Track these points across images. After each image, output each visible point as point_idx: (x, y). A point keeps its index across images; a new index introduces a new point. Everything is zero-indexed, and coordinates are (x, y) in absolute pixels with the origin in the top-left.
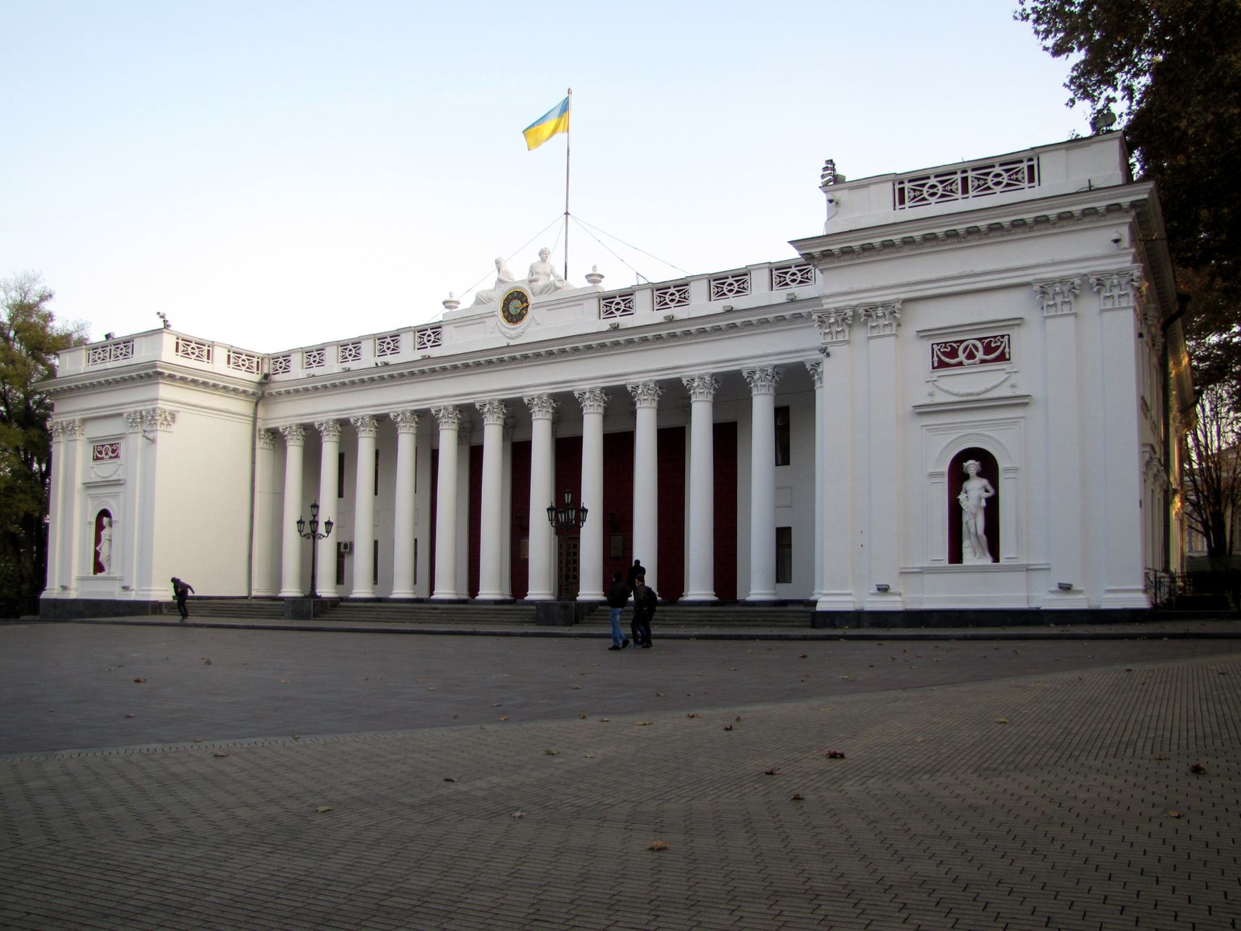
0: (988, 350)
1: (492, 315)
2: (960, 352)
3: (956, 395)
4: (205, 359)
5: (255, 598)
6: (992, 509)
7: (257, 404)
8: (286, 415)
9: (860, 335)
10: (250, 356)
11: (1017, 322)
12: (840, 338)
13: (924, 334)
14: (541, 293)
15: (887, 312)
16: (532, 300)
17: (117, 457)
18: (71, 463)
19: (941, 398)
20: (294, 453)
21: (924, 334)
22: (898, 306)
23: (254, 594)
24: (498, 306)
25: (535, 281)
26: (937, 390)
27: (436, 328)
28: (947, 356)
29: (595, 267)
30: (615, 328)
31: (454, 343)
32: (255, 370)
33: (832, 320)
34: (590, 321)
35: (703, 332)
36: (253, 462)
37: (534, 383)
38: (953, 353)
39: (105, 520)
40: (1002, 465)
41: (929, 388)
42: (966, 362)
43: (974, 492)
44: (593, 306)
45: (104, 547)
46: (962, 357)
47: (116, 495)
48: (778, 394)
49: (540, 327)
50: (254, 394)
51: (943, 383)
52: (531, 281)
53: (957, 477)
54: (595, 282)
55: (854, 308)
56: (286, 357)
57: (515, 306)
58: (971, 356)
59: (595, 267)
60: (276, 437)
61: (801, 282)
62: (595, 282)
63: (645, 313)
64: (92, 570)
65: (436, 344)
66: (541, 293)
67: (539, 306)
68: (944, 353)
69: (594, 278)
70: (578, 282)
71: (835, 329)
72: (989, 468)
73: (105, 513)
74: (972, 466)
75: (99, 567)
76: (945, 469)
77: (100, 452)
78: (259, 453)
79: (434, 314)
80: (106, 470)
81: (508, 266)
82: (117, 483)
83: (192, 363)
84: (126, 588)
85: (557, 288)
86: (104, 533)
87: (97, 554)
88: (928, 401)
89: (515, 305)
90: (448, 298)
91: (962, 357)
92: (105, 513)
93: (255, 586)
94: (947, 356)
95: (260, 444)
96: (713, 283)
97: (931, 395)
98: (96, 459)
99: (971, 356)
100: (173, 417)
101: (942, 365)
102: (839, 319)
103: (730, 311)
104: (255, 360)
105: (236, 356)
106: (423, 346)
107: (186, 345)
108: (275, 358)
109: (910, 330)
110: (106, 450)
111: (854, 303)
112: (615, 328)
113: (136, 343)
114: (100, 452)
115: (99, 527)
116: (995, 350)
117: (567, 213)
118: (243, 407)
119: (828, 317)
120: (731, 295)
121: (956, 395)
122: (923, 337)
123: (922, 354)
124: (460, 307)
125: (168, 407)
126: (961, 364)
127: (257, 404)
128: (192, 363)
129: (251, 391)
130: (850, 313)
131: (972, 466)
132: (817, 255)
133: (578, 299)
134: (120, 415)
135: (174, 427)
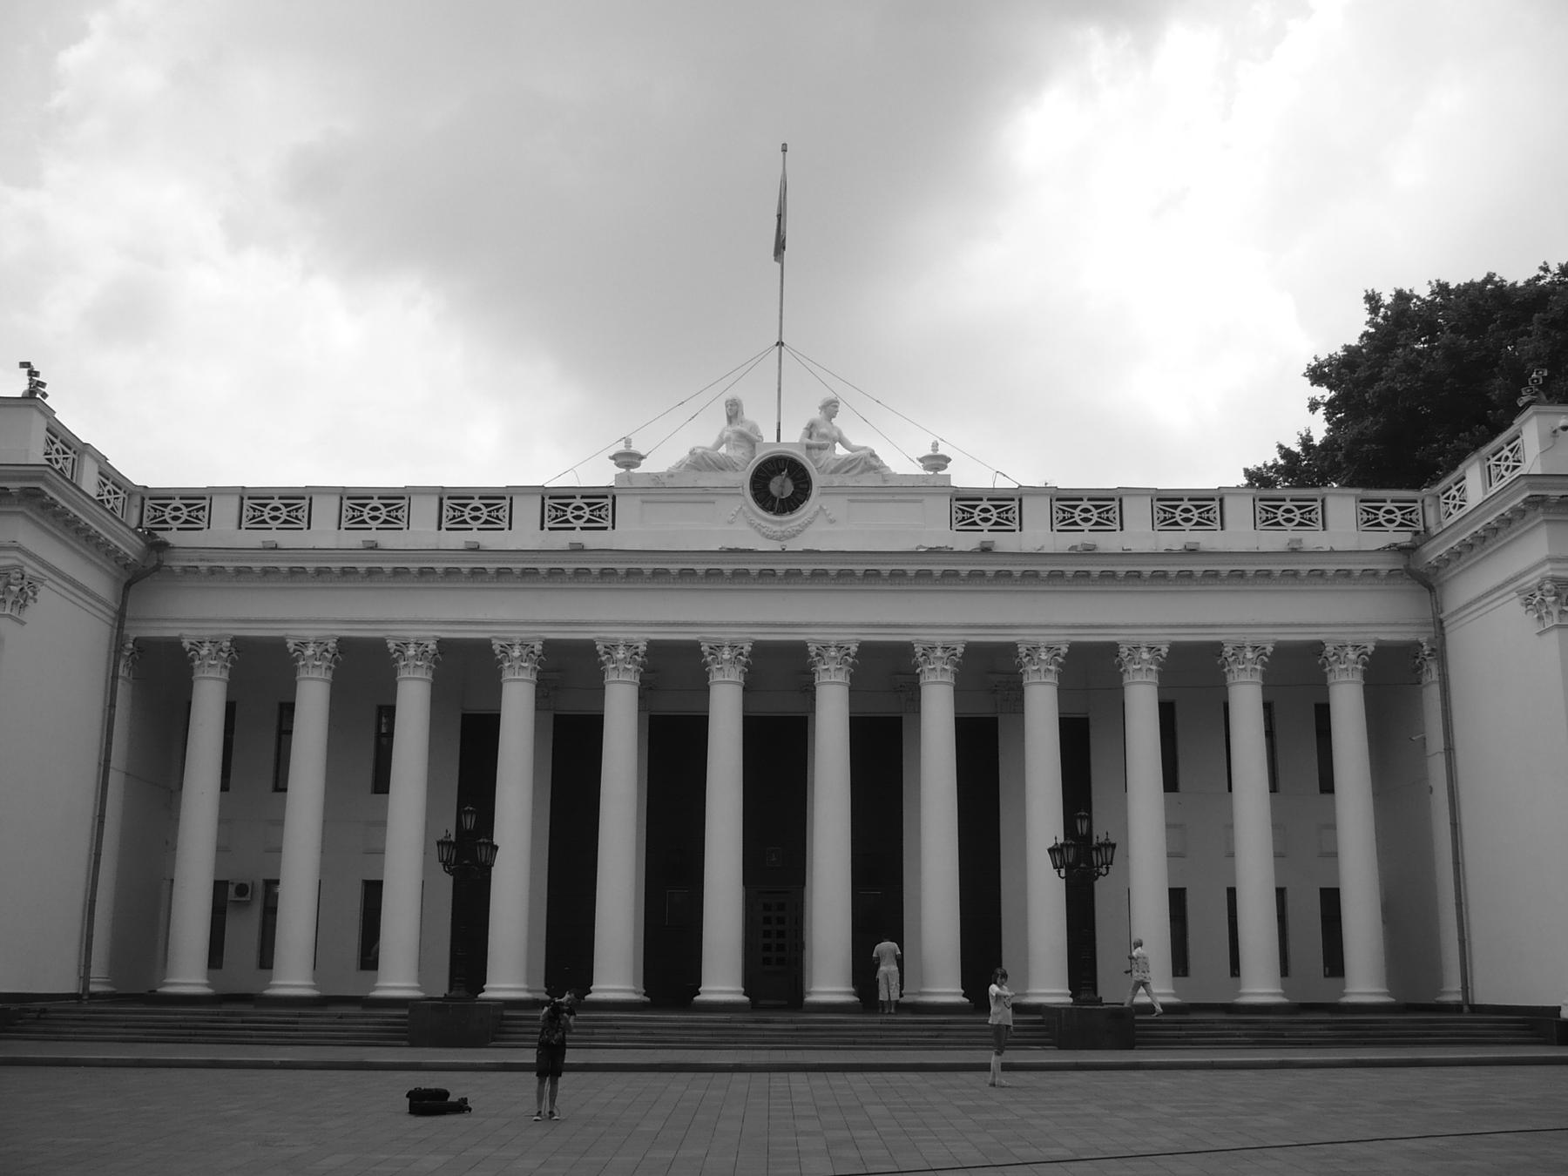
5: (93, 996)
7: (128, 586)
8: (200, 617)
14: (836, 471)
16: (817, 480)
23: (93, 988)
24: (744, 478)
25: (821, 448)
29: (935, 446)
31: (634, 531)
36: (112, 706)
37: (833, 621)
44: (941, 508)
48: (1265, 688)
49: (823, 527)
52: (809, 447)
54: (936, 469)
57: (781, 482)
59: (935, 446)
61: (1300, 524)
65: (592, 526)
66: (836, 471)
67: (828, 490)
69: (937, 462)
70: (902, 461)
79: (603, 475)
81: (749, 414)
85: (874, 468)
89: (781, 486)
90: (621, 447)
103: (1191, 551)
106: (563, 525)
108: (159, 499)
112: (986, 550)
117: (780, 344)
118: (100, 583)
120: (1187, 526)
124: (645, 467)
135: (27, 615)
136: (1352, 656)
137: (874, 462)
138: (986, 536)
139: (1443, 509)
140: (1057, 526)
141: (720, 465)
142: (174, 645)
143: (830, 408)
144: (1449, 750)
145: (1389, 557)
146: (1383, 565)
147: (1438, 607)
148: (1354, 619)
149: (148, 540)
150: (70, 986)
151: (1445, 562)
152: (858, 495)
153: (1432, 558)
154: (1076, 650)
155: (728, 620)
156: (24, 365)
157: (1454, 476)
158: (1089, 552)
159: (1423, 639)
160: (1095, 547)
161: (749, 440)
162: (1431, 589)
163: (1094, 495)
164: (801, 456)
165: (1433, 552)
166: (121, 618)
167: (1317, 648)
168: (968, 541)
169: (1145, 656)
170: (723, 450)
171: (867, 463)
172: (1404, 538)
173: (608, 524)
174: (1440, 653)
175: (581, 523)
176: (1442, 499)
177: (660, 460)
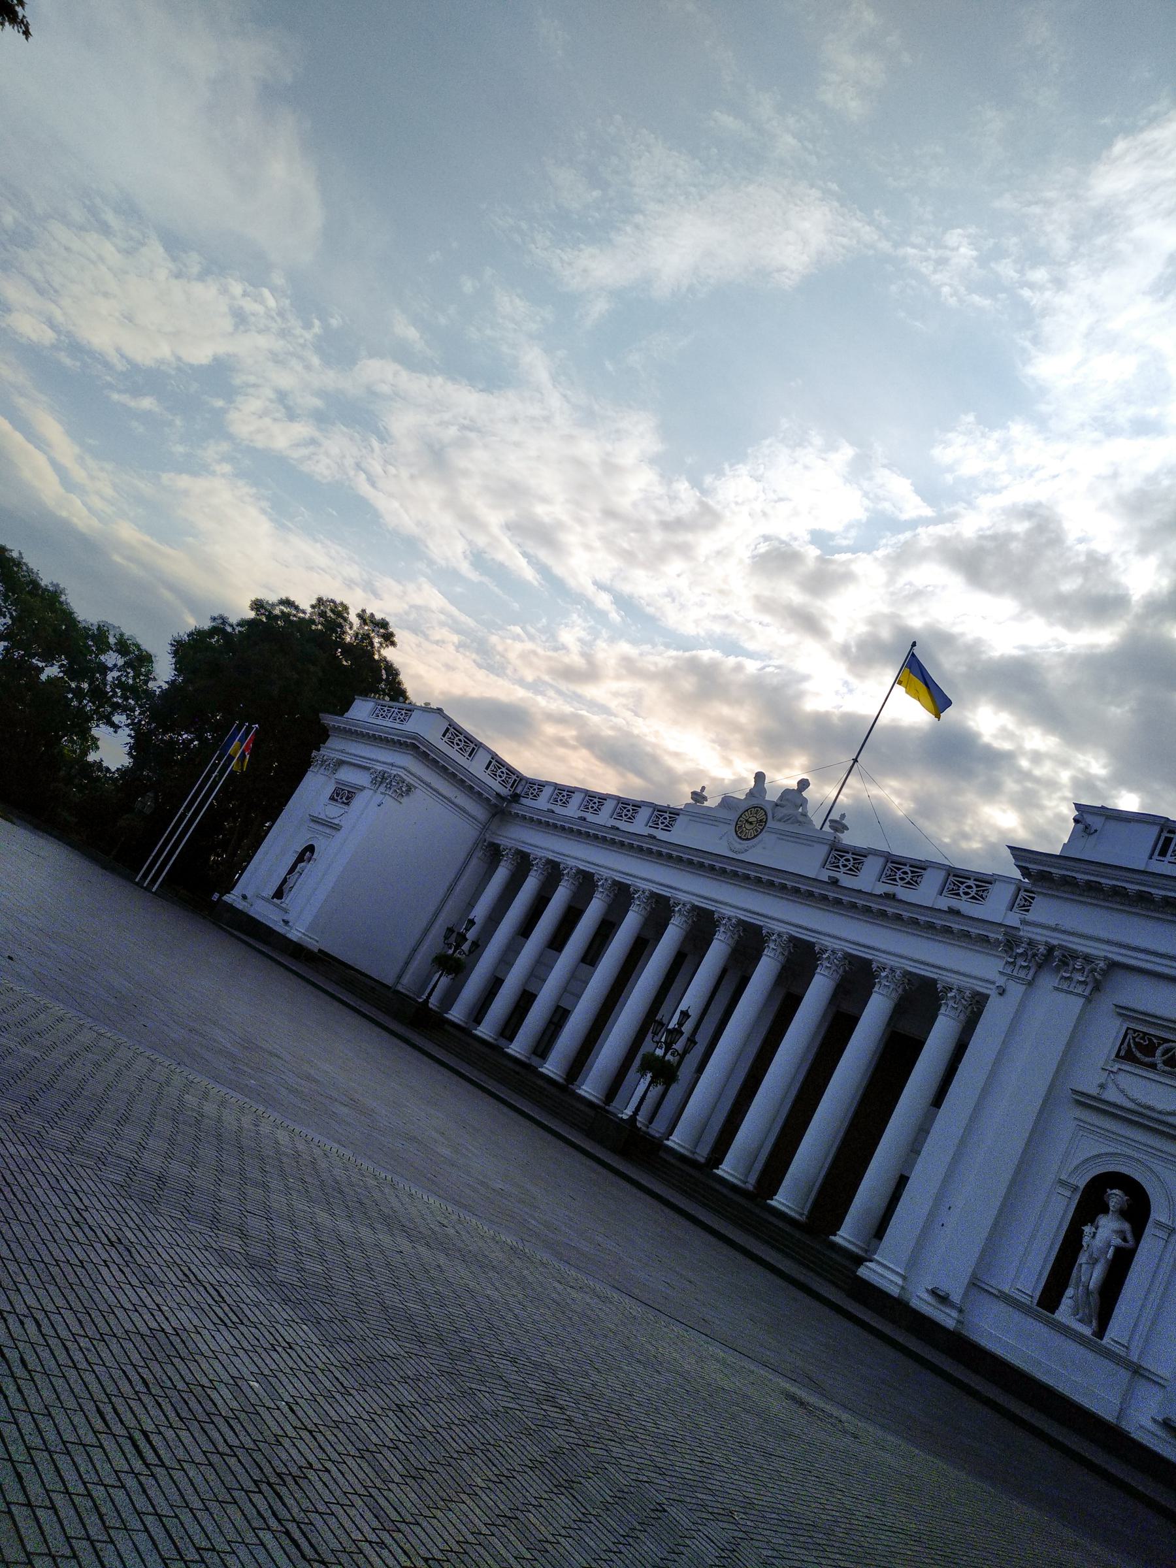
1: (726, 822)
2: (1159, 1052)
3: (1133, 1101)
4: (467, 755)
5: (399, 992)
6: (1120, 1264)
7: (494, 816)
9: (1048, 981)
10: (511, 771)
12: (1022, 975)
13: (1124, 1012)
14: (780, 820)
15: (1088, 968)
17: (347, 804)
18: (313, 791)
19: (1112, 1095)
20: (502, 874)
21: (1124, 1012)
22: (1102, 964)
23: (399, 988)
26: (1111, 1085)
27: (674, 813)
30: (834, 882)
31: (681, 835)
32: (509, 786)
33: (1020, 951)
34: (808, 863)
35: (915, 922)
38: (1150, 1050)
41: (1102, 1077)
42: (1160, 1066)
43: (1106, 1232)
45: (295, 875)
46: (1158, 1058)
47: (327, 836)
49: (766, 852)
50: (495, 806)
51: (1122, 1079)
55: (1051, 949)
56: (542, 785)
60: (494, 854)
62: (836, 830)
63: (868, 880)
64: (271, 893)
67: (774, 831)
68: (1136, 1044)
71: (1021, 962)
72: (1137, 1211)
73: (311, 849)
74: (1116, 1197)
75: (279, 894)
76: (1082, 1184)
78: (474, 861)
82: (336, 828)
83: (452, 753)
86: (301, 865)
87: (285, 881)
88: (1094, 1091)
91: (1158, 1058)
92: (311, 849)
93: (406, 980)
95: (479, 854)
96: (951, 878)
97: (1102, 1086)
98: (332, 798)
100: (409, 790)
102: (1030, 953)
104: (514, 777)
105: (497, 764)
107: (454, 732)
108: (531, 783)
109: (1106, 1002)
110: (344, 795)
111: (1055, 942)
113: (415, 714)
115: (300, 859)
117: (855, 760)
119: (1018, 946)
120: (964, 897)
121: (1133, 1101)
122: (1120, 1014)
123: (1108, 1034)
124: (706, 804)
125: (409, 779)
126: (1153, 1066)
127: (494, 816)
128: (452, 753)
129: (494, 801)
130: (1042, 949)
131: (1116, 1197)
132: (1039, 872)
133: (812, 839)
134: (369, 769)
135: (405, 800)
137: (801, 819)
140: (883, 879)
142: (498, 846)
149: (510, 797)
150: (389, 981)
152: (782, 835)
158: (891, 897)
160: (894, 895)
163: (913, 863)
166: (485, 827)
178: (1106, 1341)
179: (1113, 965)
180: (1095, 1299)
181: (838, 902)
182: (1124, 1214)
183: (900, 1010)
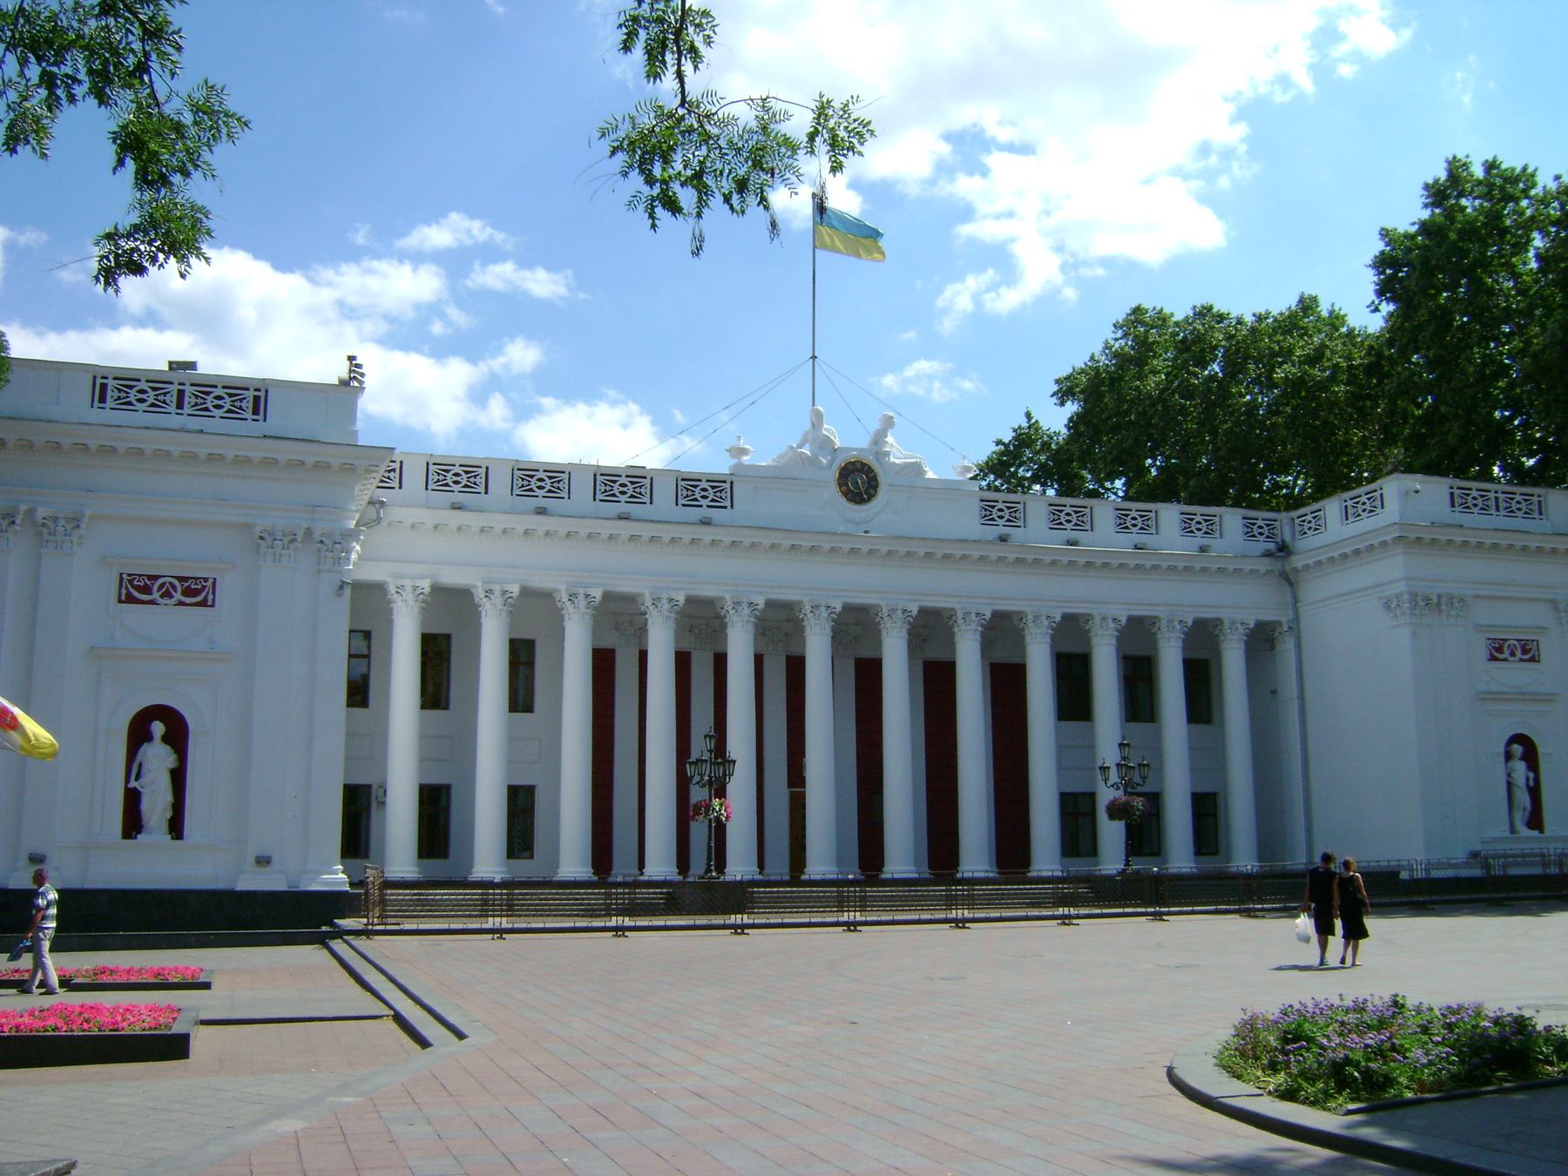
0: (1525, 651)
11: (1542, 629)
17: (203, 604)
19: (1494, 687)
21: (1480, 628)
28: (1497, 651)
37: (896, 591)
38: (1500, 650)
39: (158, 728)
40: (1541, 750)
46: (1506, 654)
53: (1508, 756)
58: (1513, 654)
75: (133, 824)
76: (1501, 750)
77: (146, 590)
80: (166, 621)
84: (263, 861)
86: (157, 756)
91: (1506, 654)
94: (1497, 651)
99: (1513, 654)
101: (1493, 658)
112: (1003, 539)
114: (146, 590)
116: (1529, 652)
117: (814, 357)
120: (1135, 530)
126: (1505, 660)
131: (1517, 749)
136: (1241, 630)
138: (1002, 530)
139: (1298, 529)
141: (812, 462)
143: (888, 422)
144: (1302, 698)
145: (1266, 560)
146: (1263, 569)
147: (1296, 600)
148: (1239, 603)
151: (1307, 567)
153: (1299, 565)
154: (1067, 618)
155: (820, 587)
156: (351, 358)
157: (1315, 506)
159: (1284, 620)
161: (825, 444)
162: (1291, 584)
164: (870, 460)
165: (1297, 561)
167: (1217, 623)
168: (993, 532)
169: (1112, 625)
170: (806, 451)
171: (916, 469)
172: (1271, 546)
173: (728, 504)
174: (1295, 627)
175: (705, 502)
176: (1297, 521)
177: (763, 453)
178: (1547, 833)
179: (1477, 597)
180: (1527, 814)
181: (1019, 561)
182: (1523, 758)
183: (987, 644)
